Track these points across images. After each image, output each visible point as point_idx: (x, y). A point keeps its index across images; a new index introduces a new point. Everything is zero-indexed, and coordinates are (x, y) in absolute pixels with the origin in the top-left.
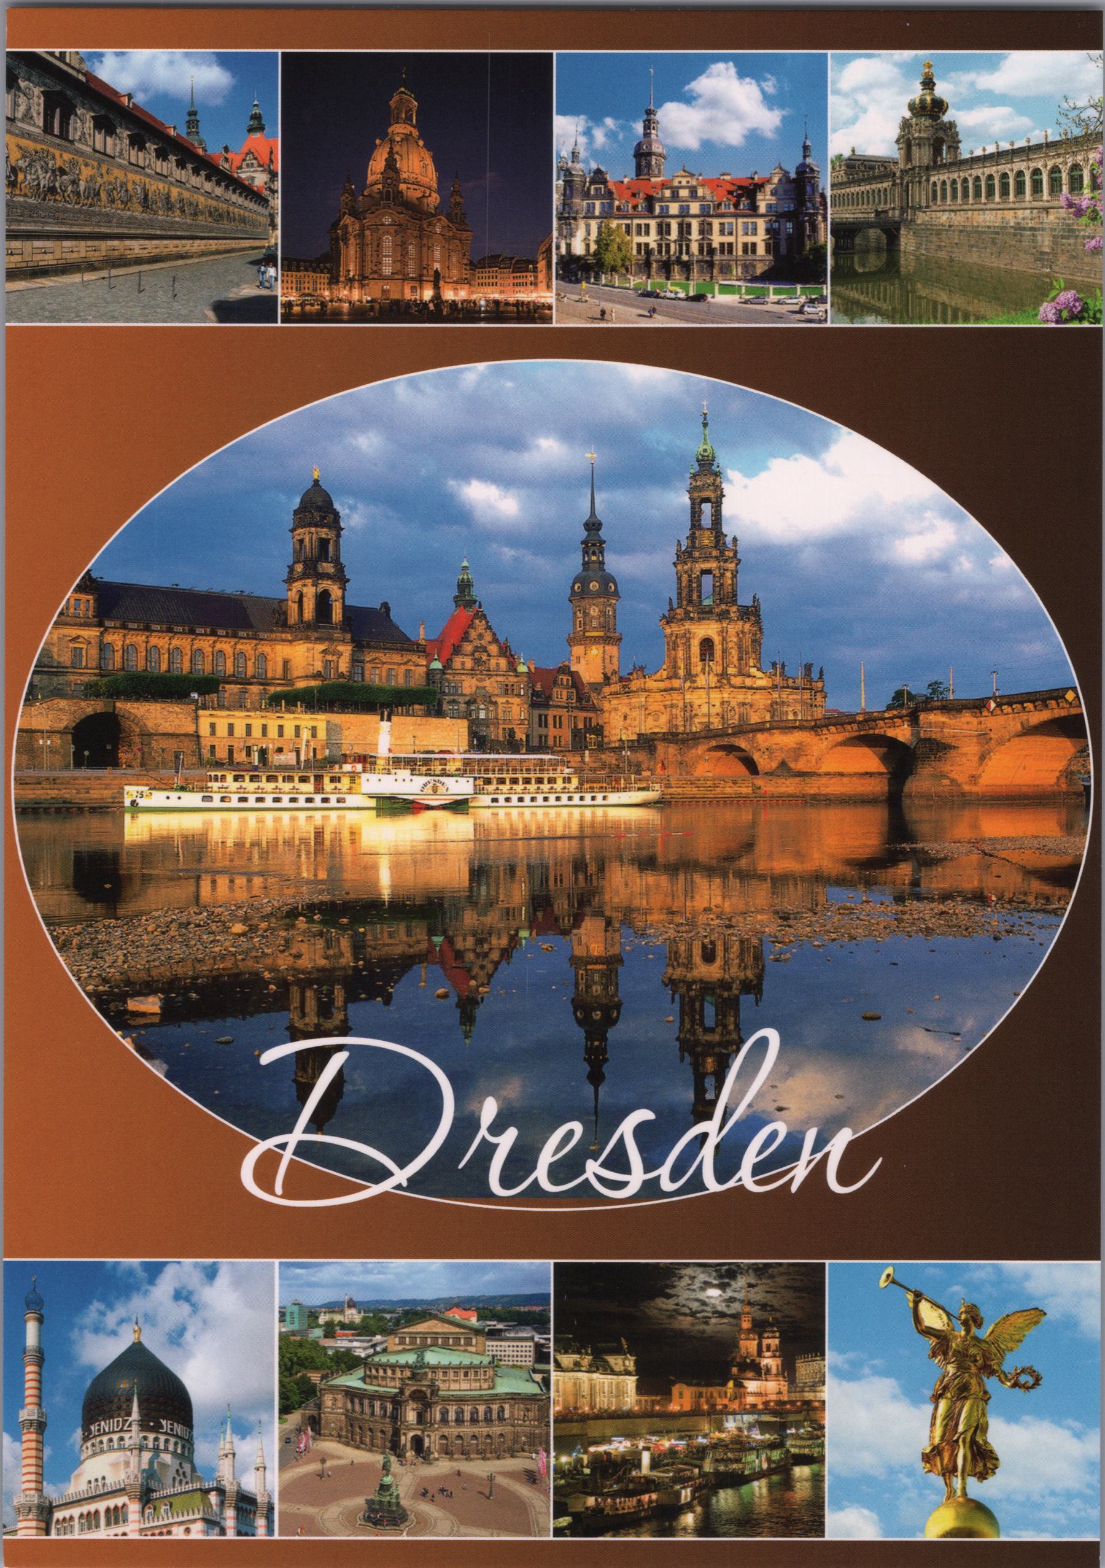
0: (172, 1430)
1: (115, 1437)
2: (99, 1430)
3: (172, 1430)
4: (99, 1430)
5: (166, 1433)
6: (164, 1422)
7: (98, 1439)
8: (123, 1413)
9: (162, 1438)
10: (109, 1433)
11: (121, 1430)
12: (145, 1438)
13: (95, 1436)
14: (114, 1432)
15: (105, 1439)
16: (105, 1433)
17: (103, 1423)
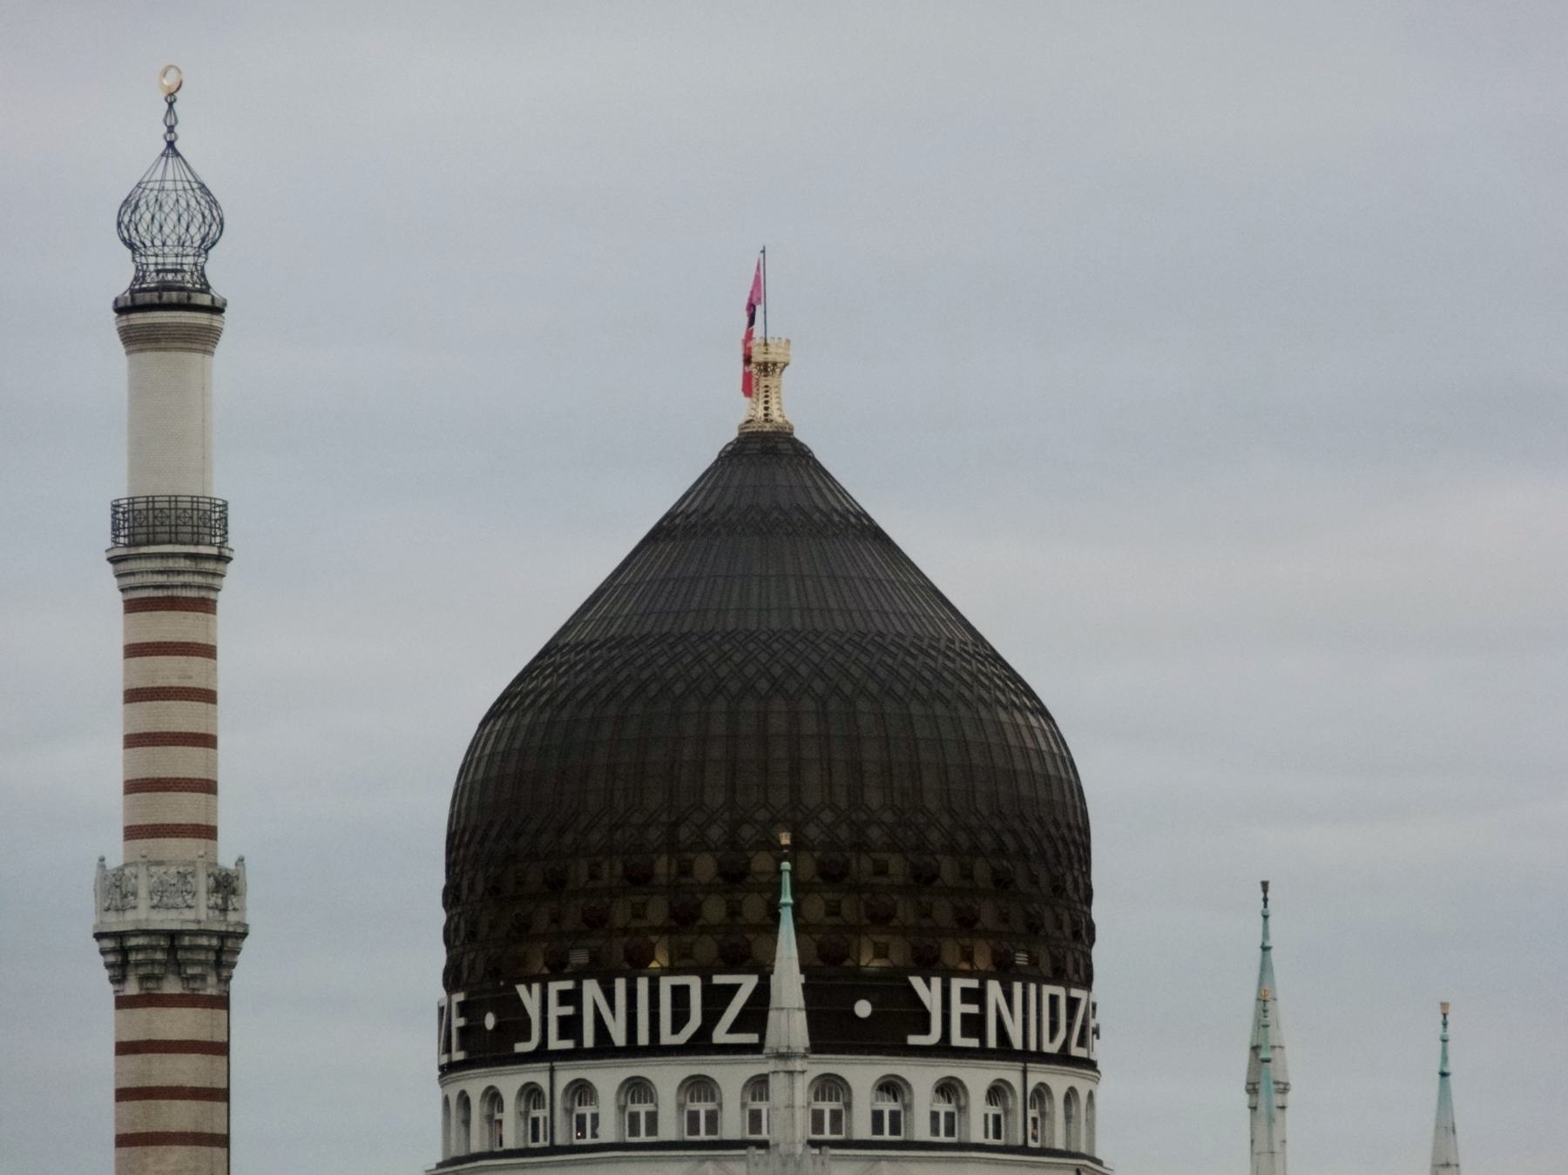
0: (974, 1025)
1: (667, 1077)
2: (570, 1027)
3: (974, 1025)
4: (570, 1027)
5: (944, 1050)
6: (929, 993)
7: (566, 1075)
8: (706, 949)
9: (922, 1077)
10: (632, 1050)
11: (701, 1044)
12: (831, 1086)
13: (542, 1054)
14: (656, 1049)
15: (607, 1078)
16: (604, 1049)
17: (591, 990)
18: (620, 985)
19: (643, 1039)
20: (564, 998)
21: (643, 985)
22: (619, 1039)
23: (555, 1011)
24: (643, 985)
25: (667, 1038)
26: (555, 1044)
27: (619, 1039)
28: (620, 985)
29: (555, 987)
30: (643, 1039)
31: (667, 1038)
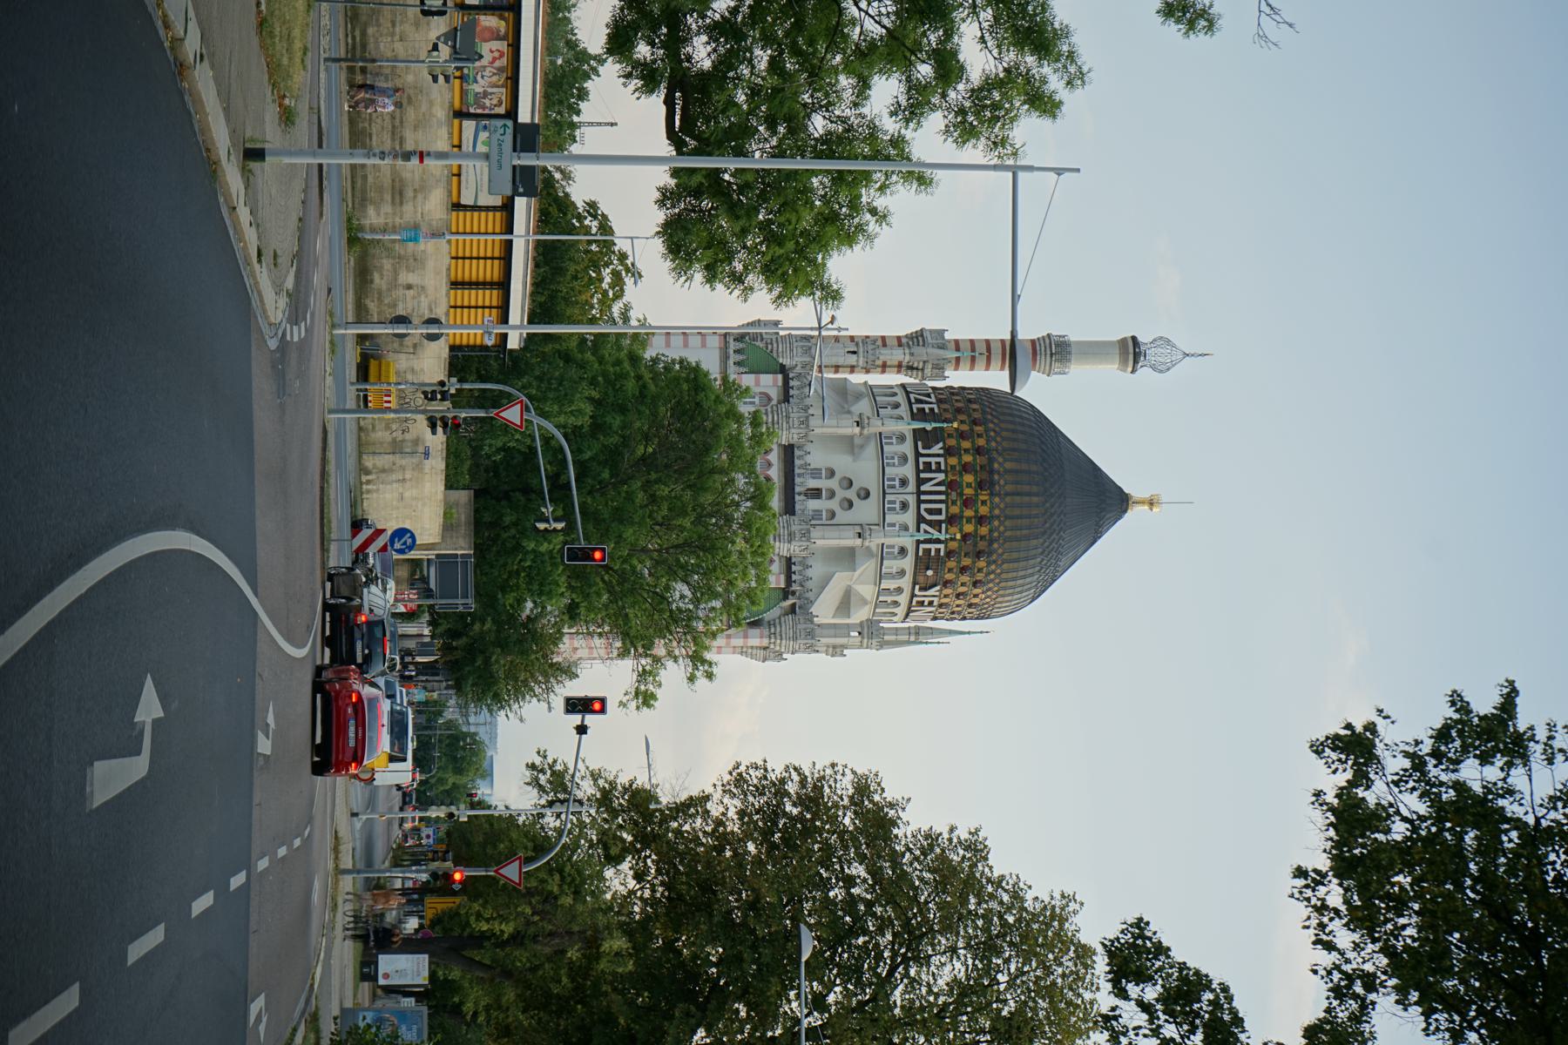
10: (919, 493)
13: (918, 455)
14: (919, 502)
16: (920, 482)
17: (941, 477)
18: (943, 488)
19: (923, 497)
20: (938, 464)
21: (943, 497)
22: (923, 488)
23: (933, 460)
24: (943, 497)
25: (923, 506)
26: (922, 460)
27: (923, 488)
28: (943, 488)
29: (941, 460)
30: (923, 497)
31: (923, 506)
